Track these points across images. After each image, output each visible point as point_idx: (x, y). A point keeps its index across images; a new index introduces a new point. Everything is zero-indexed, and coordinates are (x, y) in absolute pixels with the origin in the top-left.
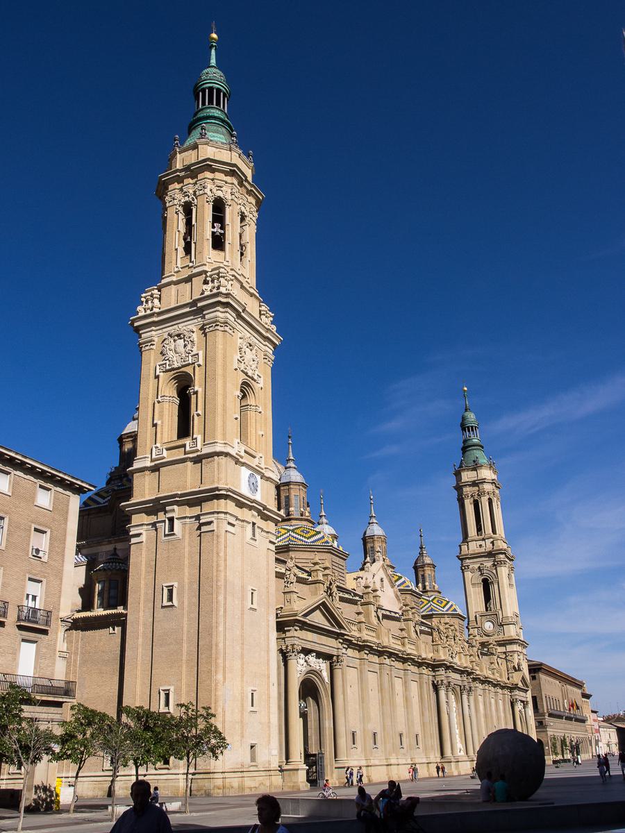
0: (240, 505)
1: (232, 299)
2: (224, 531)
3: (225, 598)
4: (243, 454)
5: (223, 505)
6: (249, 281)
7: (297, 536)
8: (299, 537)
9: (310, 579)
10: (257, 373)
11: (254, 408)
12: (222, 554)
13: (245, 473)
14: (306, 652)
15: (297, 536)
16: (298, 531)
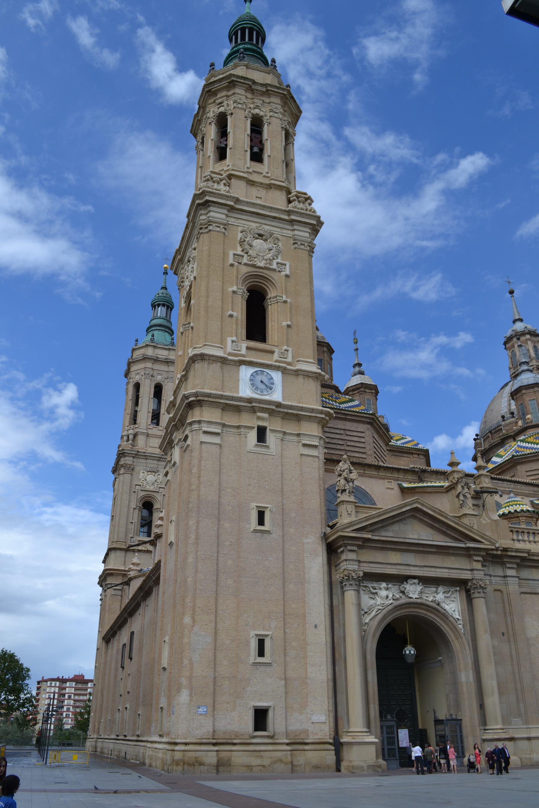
0: (237, 409)
1: (209, 196)
2: (198, 443)
3: (198, 522)
4: (244, 351)
5: (195, 415)
6: (269, 175)
7: (527, 445)
8: (530, 445)
9: (446, 484)
10: (275, 262)
11: (275, 299)
12: (195, 470)
13: (246, 372)
14: (401, 579)
15: (527, 445)
16: (529, 440)
